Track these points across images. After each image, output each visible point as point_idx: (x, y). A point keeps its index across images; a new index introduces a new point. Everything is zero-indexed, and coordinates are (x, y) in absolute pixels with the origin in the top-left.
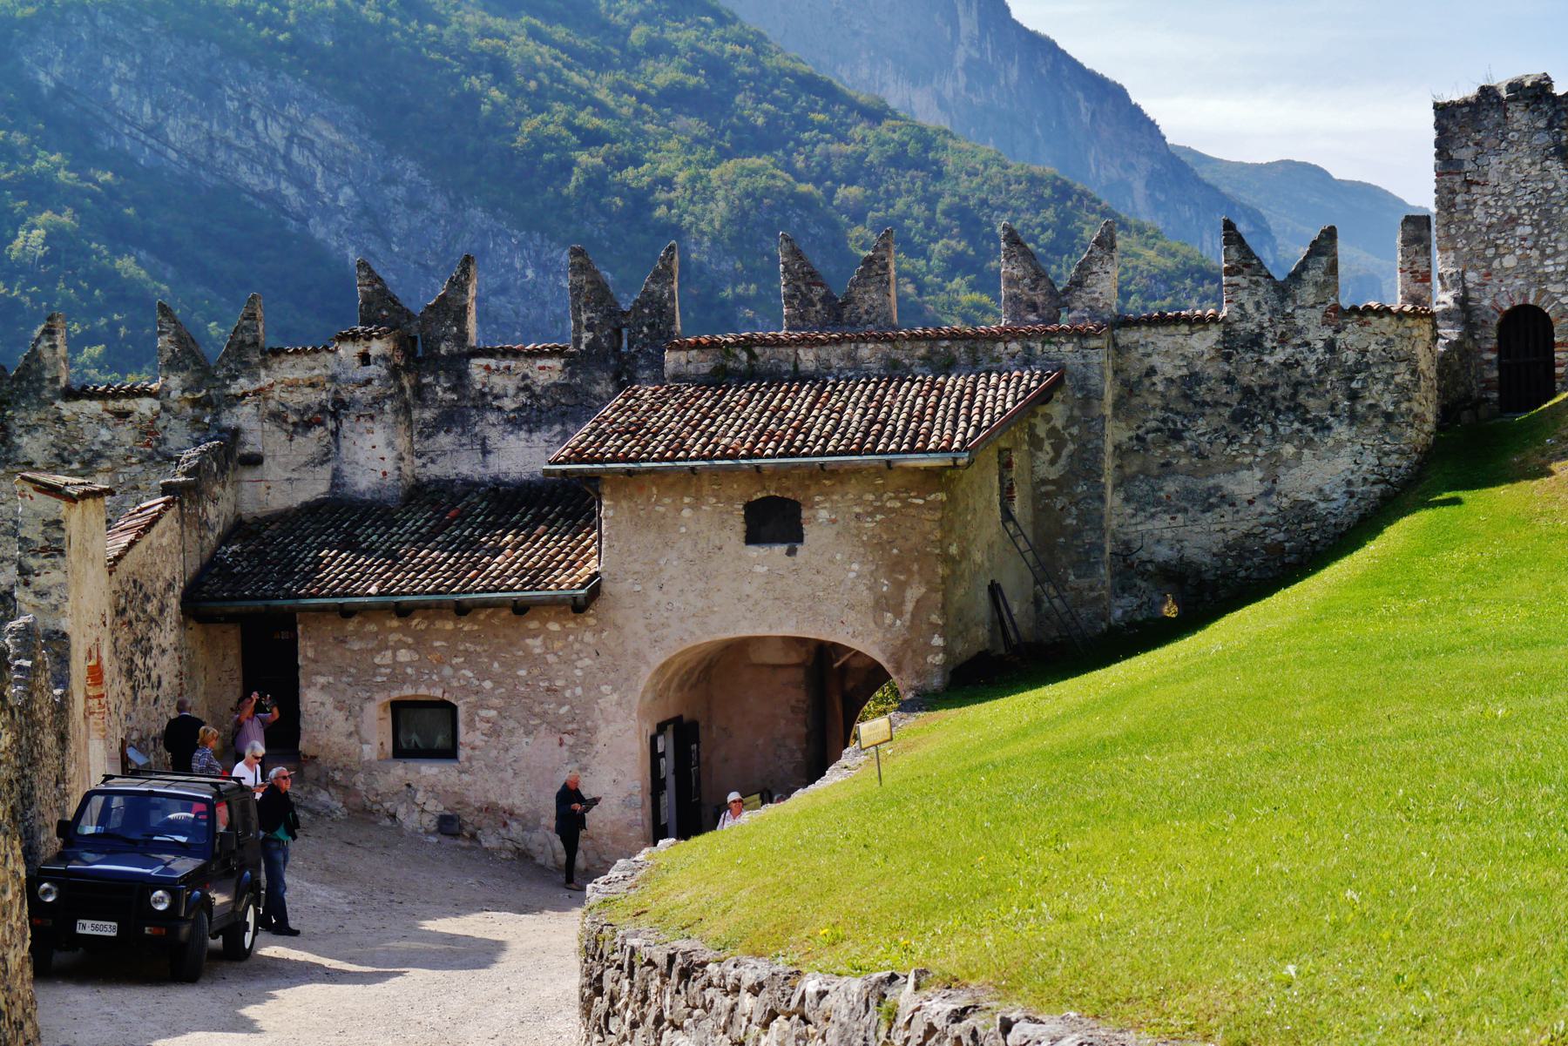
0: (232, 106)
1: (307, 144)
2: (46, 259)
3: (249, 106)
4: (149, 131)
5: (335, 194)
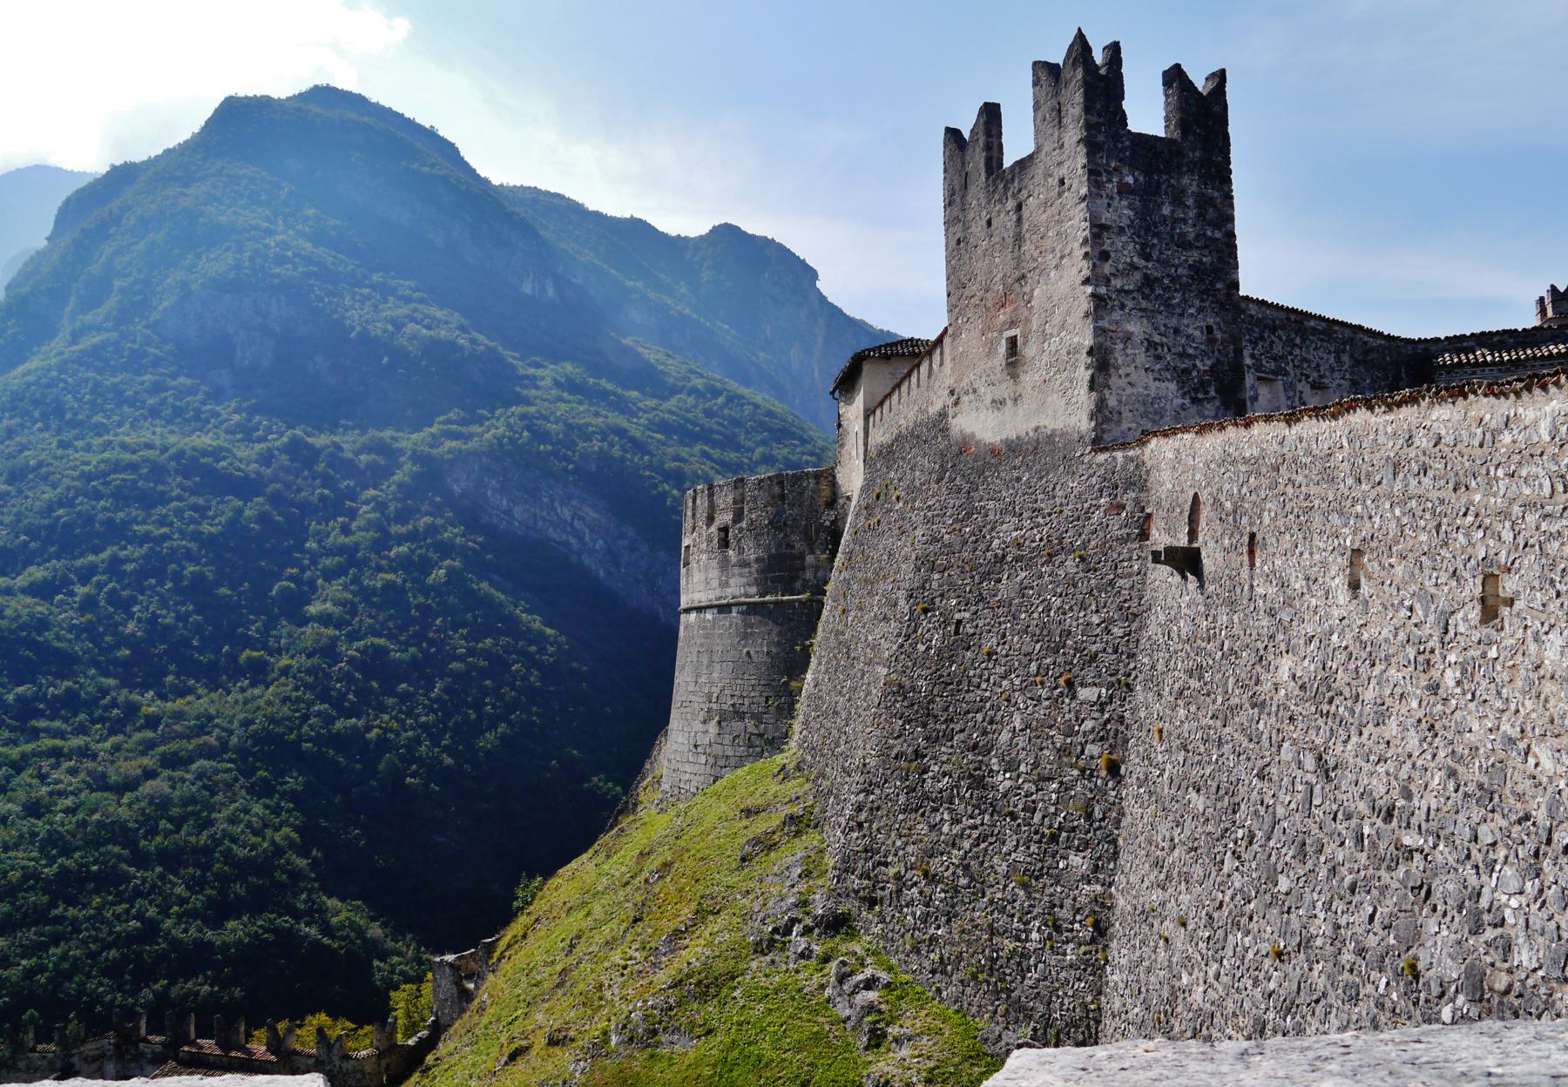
0: (545, 500)
1: (583, 519)
3: (553, 501)
4: (505, 513)
5: (595, 541)
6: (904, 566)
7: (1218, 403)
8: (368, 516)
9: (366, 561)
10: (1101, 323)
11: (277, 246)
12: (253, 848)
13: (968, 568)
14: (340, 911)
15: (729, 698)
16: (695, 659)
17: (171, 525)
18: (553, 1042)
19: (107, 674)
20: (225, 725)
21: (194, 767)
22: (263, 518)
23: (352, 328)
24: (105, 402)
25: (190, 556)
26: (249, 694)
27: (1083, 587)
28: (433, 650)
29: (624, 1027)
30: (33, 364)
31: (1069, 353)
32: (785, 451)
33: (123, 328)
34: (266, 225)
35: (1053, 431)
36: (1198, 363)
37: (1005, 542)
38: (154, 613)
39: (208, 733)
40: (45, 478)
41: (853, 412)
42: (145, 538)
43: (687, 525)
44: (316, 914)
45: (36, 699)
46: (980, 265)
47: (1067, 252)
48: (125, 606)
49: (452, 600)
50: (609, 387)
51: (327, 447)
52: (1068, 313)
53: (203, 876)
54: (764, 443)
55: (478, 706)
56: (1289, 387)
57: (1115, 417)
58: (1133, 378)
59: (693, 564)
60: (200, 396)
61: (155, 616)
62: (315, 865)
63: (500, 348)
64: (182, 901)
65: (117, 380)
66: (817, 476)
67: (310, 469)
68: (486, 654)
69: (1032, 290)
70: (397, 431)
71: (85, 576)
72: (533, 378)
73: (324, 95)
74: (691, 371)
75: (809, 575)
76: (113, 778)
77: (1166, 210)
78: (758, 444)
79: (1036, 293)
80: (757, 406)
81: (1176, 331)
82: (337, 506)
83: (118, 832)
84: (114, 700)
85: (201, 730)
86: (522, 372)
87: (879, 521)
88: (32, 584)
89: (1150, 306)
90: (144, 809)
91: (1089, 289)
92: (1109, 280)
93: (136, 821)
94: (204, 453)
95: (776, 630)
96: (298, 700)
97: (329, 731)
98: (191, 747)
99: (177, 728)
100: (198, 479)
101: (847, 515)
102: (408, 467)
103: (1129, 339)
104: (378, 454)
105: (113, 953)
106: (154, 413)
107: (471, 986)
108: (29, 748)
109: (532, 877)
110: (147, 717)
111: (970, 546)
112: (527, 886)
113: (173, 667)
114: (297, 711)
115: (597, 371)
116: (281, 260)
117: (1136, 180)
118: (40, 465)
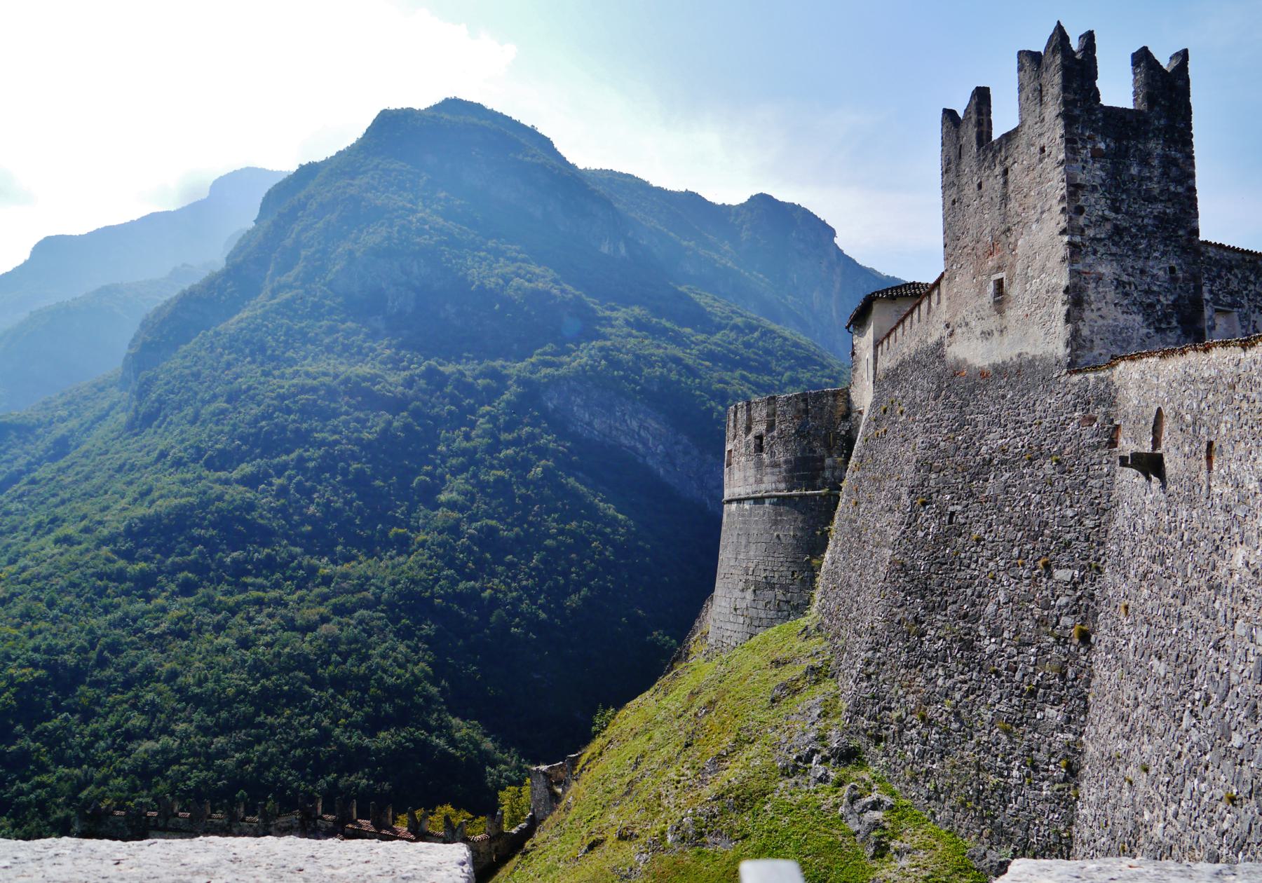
0: (618, 414)
1: (646, 429)
2: (542, 479)
3: (624, 415)
6: (906, 468)
7: (1179, 332)
8: (484, 426)
9: (482, 461)
10: (1075, 267)
11: (418, 221)
12: (399, 677)
13: (960, 470)
14: (463, 728)
15: (762, 572)
16: (735, 540)
17: (340, 433)
18: (622, 837)
19: (295, 545)
20: (379, 584)
21: (356, 615)
22: (407, 428)
23: (473, 283)
24: (294, 341)
25: (354, 457)
26: (396, 561)
27: (1059, 486)
28: (532, 530)
29: (678, 828)
30: (245, 314)
31: (1048, 292)
32: (808, 375)
33: (307, 286)
34: (409, 205)
35: (1034, 357)
36: (1162, 298)
37: (992, 448)
38: (328, 499)
39: (367, 590)
40: (252, 398)
41: (865, 342)
42: (322, 443)
43: (730, 434)
44: (443, 729)
45: (246, 561)
46: (971, 220)
47: (1046, 208)
48: (308, 493)
49: (547, 492)
50: (668, 325)
51: (453, 373)
52: (1048, 259)
53: (362, 698)
54: (791, 368)
55: (566, 574)
56: (1244, 318)
57: (1088, 345)
58: (1104, 311)
59: (735, 465)
60: (361, 336)
61: (329, 501)
62: (443, 692)
63: (584, 296)
64: (348, 716)
65: (303, 325)
66: (835, 394)
67: (441, 390)
68: (572, 533)
69: (1017, 240)
70: (506, 361)
71: (280, 471)
72: (609, 319)
73: (452, 105)
74: (733, 312)
75: (827, 474)
76: (299, 622)
77: (1134, 170)
78: (787, 369)
79: (1019, 243)
80: (785, 339)
81: (1143, 272)
82: (462, 418)
83: (302, 662)
84: (300, 563)
85: (362, 587)
86: (600, 314)
87: (886, 431)
88: (244, 476)
89: (1119, 251)
90: (321, 646)
91: (1066, 239)
92: (1083, 231)
93: (315, 654)
94: (365, 379)
95: (801, 518)
96: (432, 566)
97: (454, 590)
98: (354, 600)
99: (344, 585)
100: (360, 399)
101: (859, 426)
102: (514, 388)
103: (1101, 279)
104: (491, 378)
105: (299, 752)
106: (329, 349)
107: (560, 790)
108: (241, 597)
109: (606, 708)
110: (323, 577)
111: (962, 452)
112: (602, 715)
113: (341, 540)
114: (430, 575)
115: (658, 312)
116: (420, 232)
117: (1108, 146)
118: (249, 388)
